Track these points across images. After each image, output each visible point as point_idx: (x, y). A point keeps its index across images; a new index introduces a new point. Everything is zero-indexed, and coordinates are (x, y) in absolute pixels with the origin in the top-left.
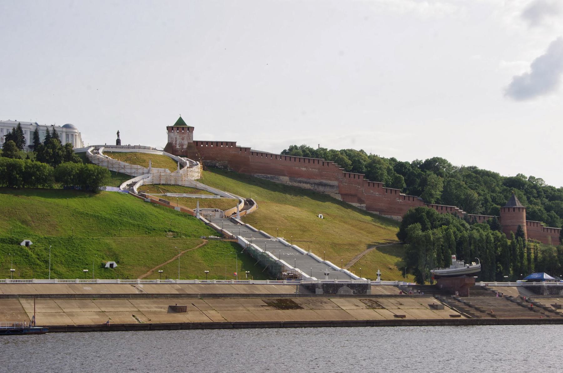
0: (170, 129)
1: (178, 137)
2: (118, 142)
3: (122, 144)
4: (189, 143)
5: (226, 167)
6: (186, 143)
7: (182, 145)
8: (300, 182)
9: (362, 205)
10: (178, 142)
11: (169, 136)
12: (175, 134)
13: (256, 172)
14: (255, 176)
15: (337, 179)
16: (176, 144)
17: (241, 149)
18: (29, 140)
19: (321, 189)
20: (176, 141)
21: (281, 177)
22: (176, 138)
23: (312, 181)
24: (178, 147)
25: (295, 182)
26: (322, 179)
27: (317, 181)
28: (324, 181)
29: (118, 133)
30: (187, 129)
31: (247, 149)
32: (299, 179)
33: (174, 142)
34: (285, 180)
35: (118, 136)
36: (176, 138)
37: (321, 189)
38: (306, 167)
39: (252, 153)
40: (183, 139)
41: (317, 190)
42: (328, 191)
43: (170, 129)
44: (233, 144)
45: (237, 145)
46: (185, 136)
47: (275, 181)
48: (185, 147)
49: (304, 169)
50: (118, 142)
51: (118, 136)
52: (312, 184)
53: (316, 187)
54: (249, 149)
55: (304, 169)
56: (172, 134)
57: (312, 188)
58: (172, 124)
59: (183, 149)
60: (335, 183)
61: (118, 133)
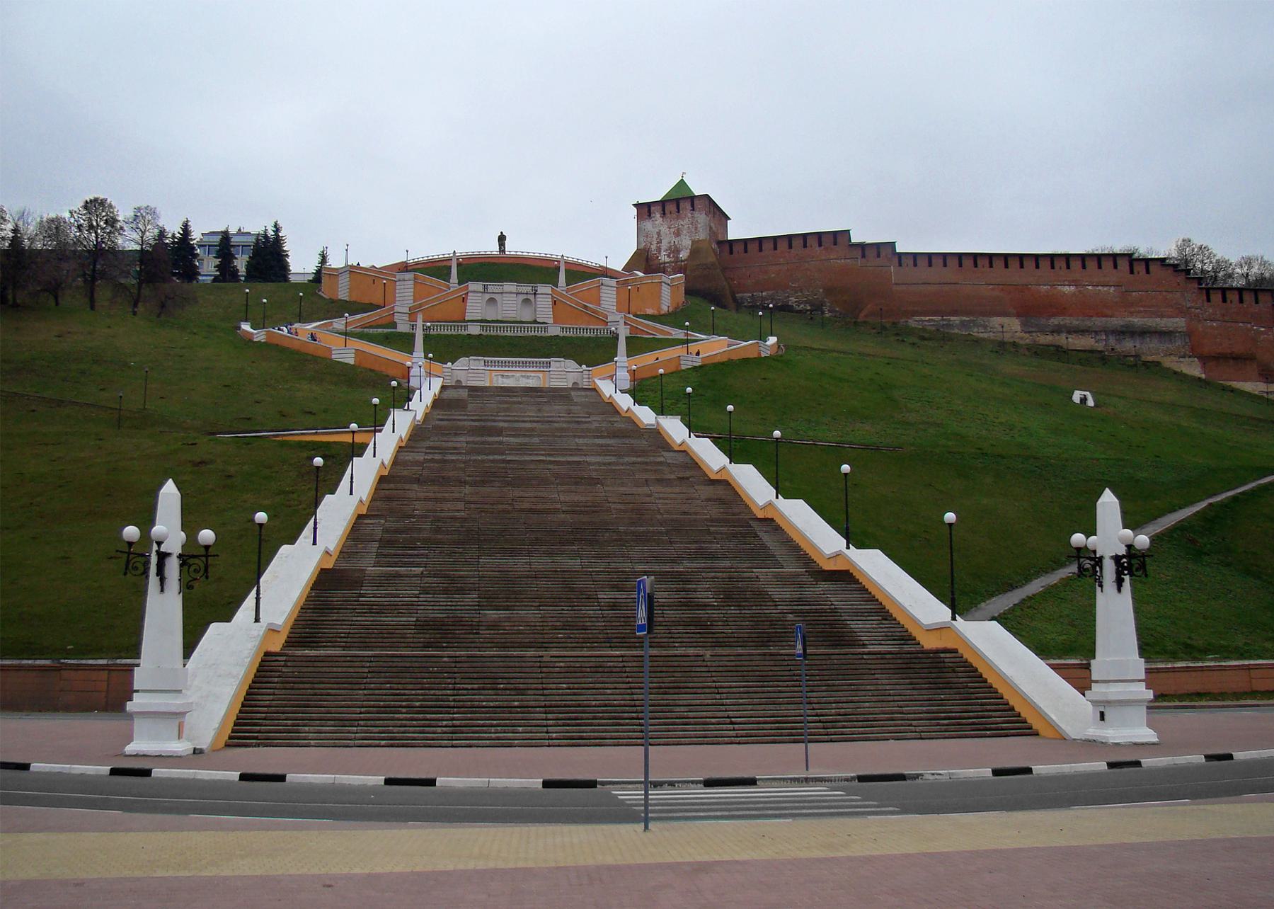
0: (644, 210)
1: (664, 229)
5: (818, 307)
6: (686, 242)
7: (675, 251)
8: (1057, 330)
10: (664, 245)
12: (658, 223)
13: (914, 313)
14: (912, 323)
15: (1181, 311)
16: (659, 249)
17: (862, 247)
18: (208, 266)
19: (1128, 345)
21: (996, 321)
22: (659, 233)
23: (1098, 322)
24: (664, 257)
25: (1043, 331)
26: (1132, 314)
27: (1116, 322)
28: (1137, 321)
29: (502, 239)
30: (688, 205)
31: (884, 250)
32: (1055, 321)
33: (654, 247)
34: (1011, 327)
36: (659, 233)
37: (1128, 345)
38: (1075, 283)
40: (678, 234)
41: (1118, 348)
42: (1151, 349)
43: (644, 210)
44: (839, 238)
46: (685, 223)
47: (977, 333)
48: (684, 255)
49: (1066, 289)
52: (1096, 332)
53: (1112, 341)
54: (893, 245)
55: (1066, 289)
56: (648, 225)
57: (1100, 347)
59: (677, 260)
60: (1179, 323)
61: (502, 239)
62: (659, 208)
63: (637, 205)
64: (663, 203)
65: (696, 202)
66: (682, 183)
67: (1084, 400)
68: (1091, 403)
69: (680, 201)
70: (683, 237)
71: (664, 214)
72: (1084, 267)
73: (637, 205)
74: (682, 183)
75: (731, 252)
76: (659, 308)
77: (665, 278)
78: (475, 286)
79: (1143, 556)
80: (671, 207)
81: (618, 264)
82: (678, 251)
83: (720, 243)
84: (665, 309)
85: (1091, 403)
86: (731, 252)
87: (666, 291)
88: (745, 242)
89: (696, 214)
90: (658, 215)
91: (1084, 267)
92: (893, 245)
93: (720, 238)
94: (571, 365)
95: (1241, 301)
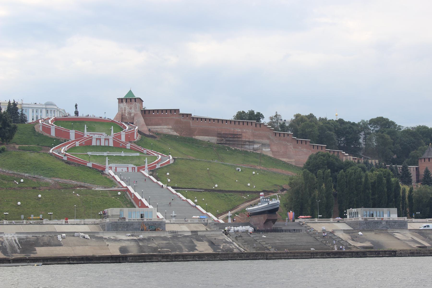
1: (127, 107)
2: (77, 113)
3: (80, 115)
7: (130, 114)
9: (291, 160)
10: (127, 112)
11: (119, 106)
15: (269, 139)
16: (125, 112)
17: (183, 115)
20: (125, 110)
22: (125, 108)
29: (76, 106)
30: (134, 100)
33: (123, 112)
35: (76, 108)
36: (125, 108)
39: (193, 118)
40: (131, 109)
43: (121, 100)
45: (181, 112)
50: (77, 113)
51: (76, 108)
54: (191, 114)
56: (121, 105)
58: (122, 96)
61: (76, 106)
62: (125, 100)
65: (136, 100)
66: (130, 92)
67: (239, 170)
68: (240, 170)
71: (126, 101)
72: (243, 124)
74: (130, 92)
76: (134, 139)
85: (240, 170)
89: (136, 103)
91: (243, 124)
92: (191, 114)
95: (284, 136)
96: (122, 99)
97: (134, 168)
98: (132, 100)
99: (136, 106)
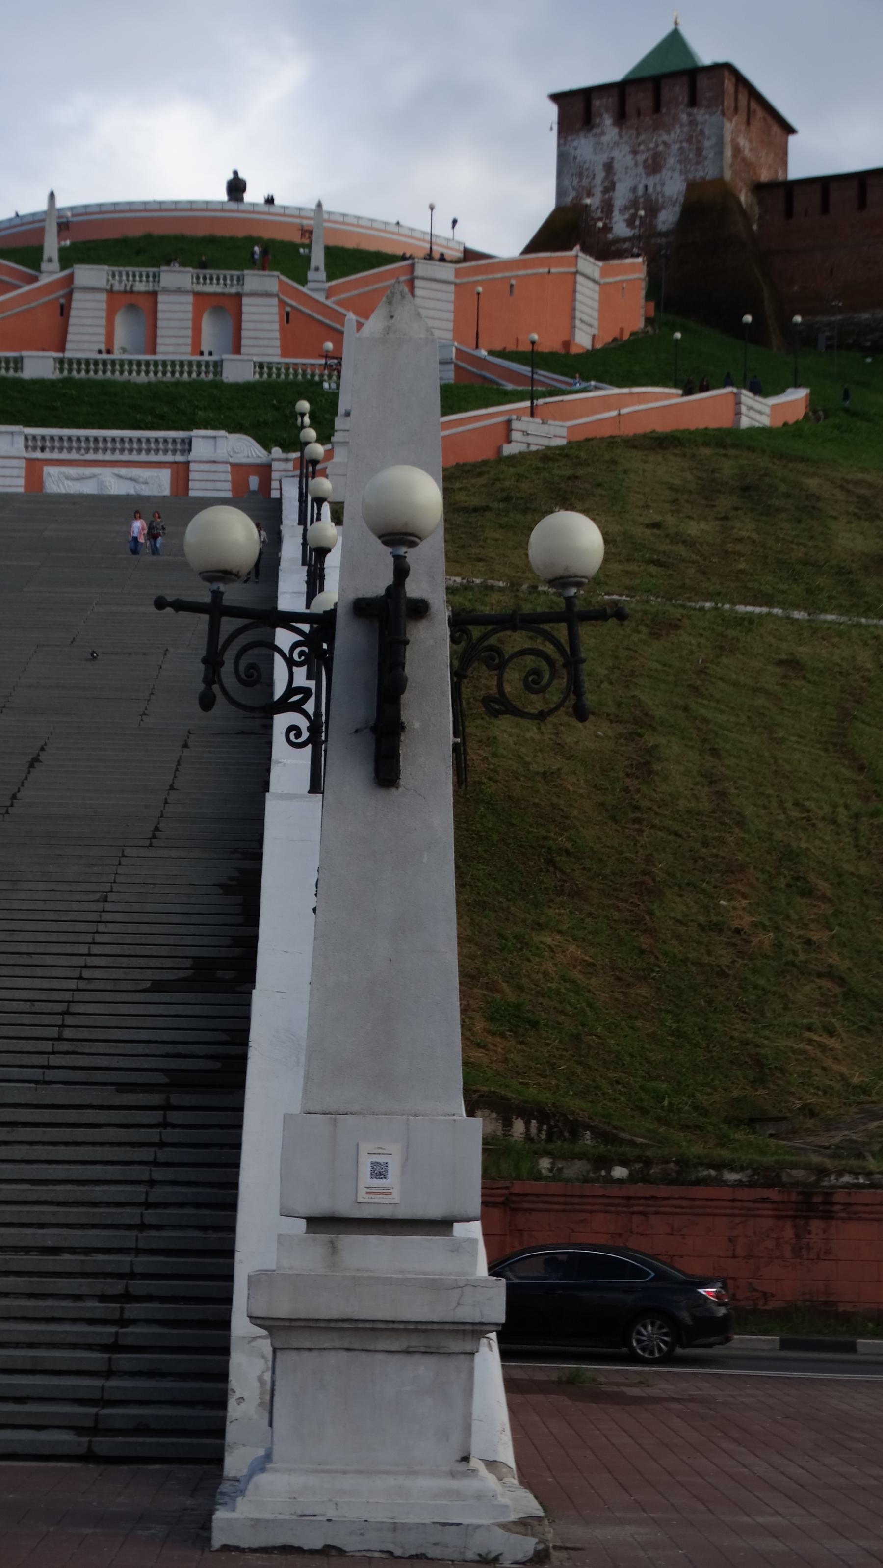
0: (577, 110)
1: (622, 157)
4: (691, 186)
6: (673, 186)
11: (562, 158)
12: (608, 143)
16: (608, 207)
20: (609, 188)
22: (609, 167)
24: (620, 228)
29: (236, 187)
30: (678, 91)
36: (609, 167)
40: (654, 166)
43: (577, 110)
46: (672, 138)
48: (667, 219)
56: (584, 147)
61: (236, 187)
62: (612, 100)
63: (556, 97)
64: (619, 91)
65: (703, 83)
69: (672, 88)
70: (666, 173)
71: (621, 118)
73: (556, 97)
75: (789, 213)
77: (588, 265)
78: (88, 275)
79: (572, 616)
80: (641, 99)
81: (506, 241)
82: (653, 209)
83: (760, 189)
84: (583, 340)
86: (789, 213)
87: (587, 299)
88: (825, 185)
89: (701, 115)
90: (608, 121)
93: (765, 176)
94: (243, 448)
96: (587, 95)
97: (264, 471)
98: (666, 94)
99: (694, 138)
